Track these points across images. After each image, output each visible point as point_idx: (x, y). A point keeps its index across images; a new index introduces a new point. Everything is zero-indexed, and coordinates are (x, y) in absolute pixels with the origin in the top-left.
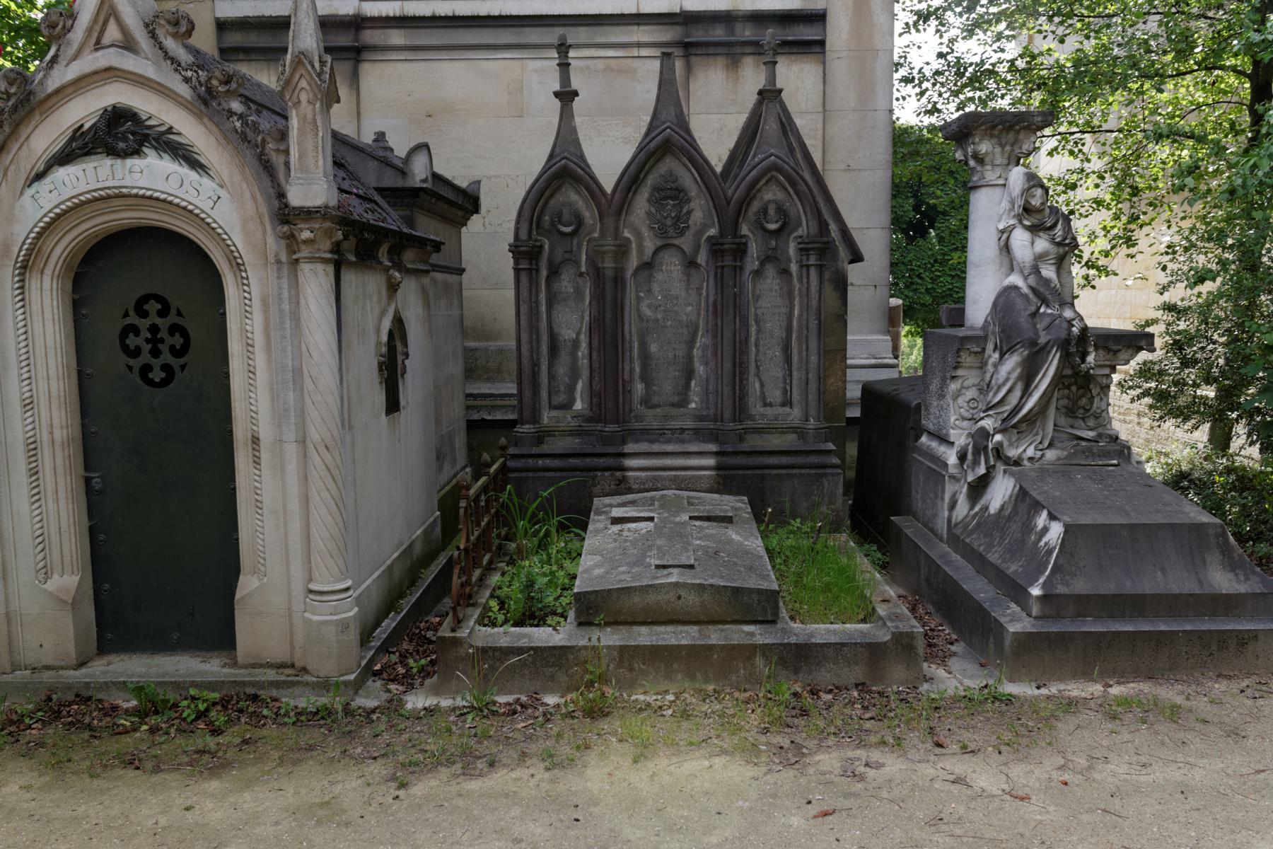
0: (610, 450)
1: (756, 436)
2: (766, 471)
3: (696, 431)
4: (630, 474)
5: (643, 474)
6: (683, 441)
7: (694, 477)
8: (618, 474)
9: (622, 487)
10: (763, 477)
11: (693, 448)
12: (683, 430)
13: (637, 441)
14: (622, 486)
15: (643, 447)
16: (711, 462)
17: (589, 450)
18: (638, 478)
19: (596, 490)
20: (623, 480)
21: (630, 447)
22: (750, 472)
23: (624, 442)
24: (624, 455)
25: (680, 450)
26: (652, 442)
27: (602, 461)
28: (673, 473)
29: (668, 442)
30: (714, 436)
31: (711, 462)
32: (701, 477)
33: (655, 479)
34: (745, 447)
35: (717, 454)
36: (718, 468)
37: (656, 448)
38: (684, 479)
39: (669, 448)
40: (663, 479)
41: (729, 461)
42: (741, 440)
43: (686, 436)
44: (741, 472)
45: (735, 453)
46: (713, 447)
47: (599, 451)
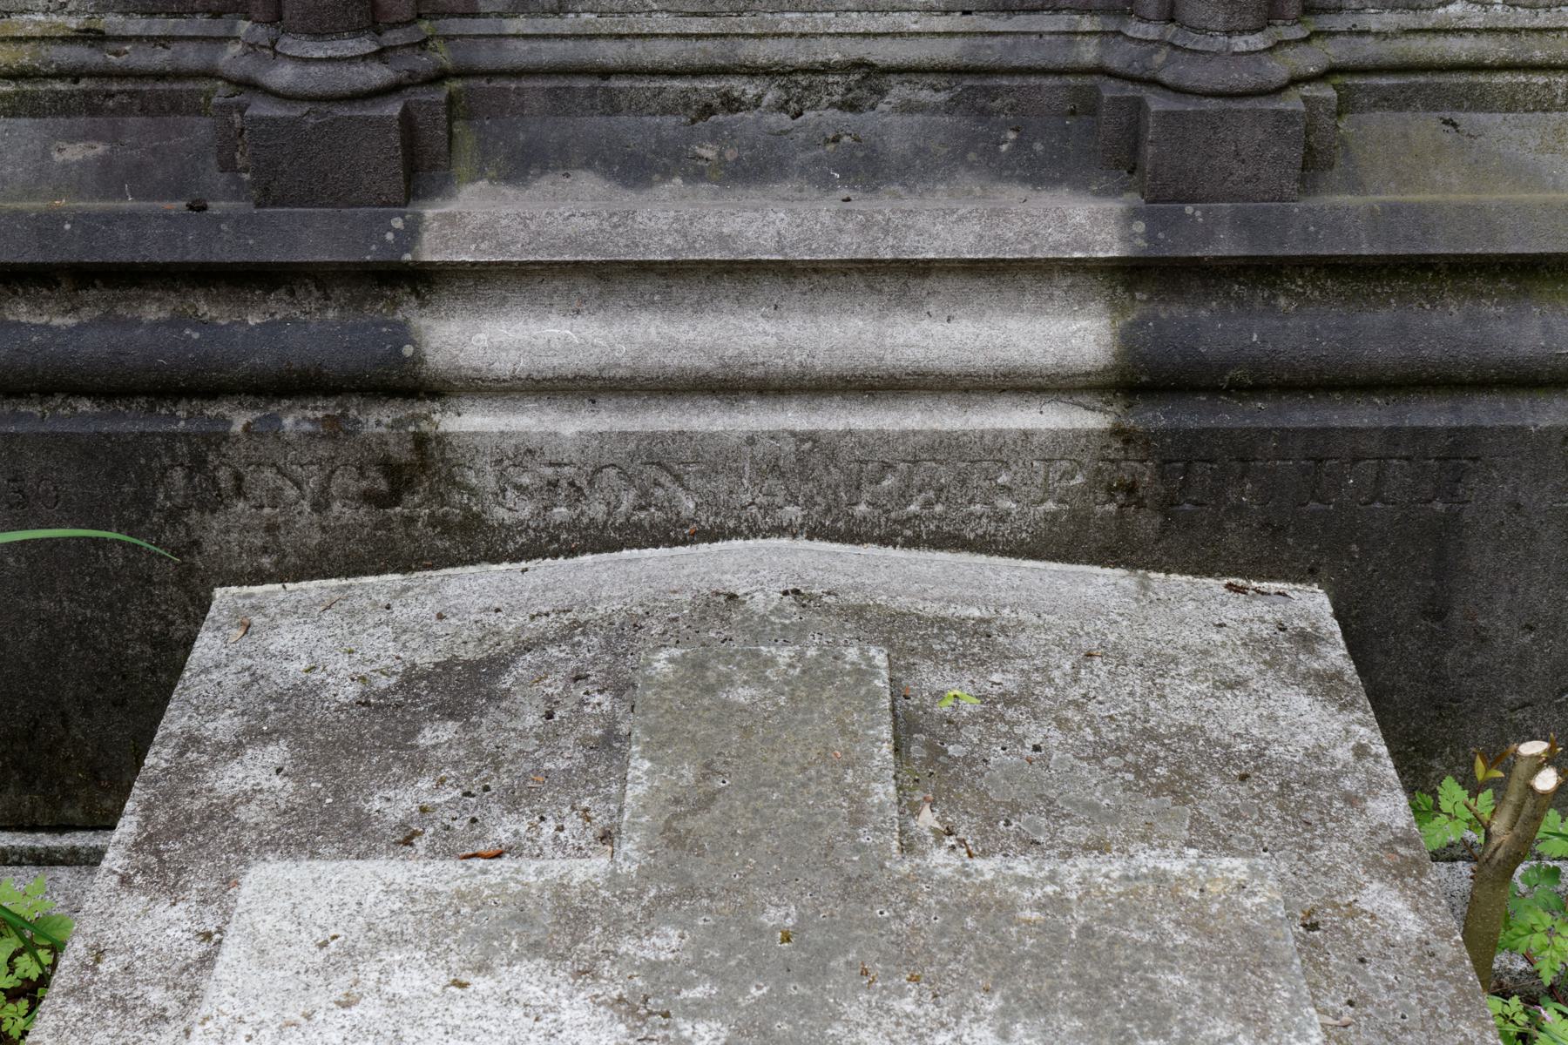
0: (313, 237)
1: (1423, 126)
2: (1483, 411)
3: (968, 79)
4: (468, 422)
5: (569, 426)
6: (864, 168)
7: (944, 446)
8: (378, 420)
9: (413, 513)
10: (1459, 453)
11: (945, 224)
12: (872, 75)
13: (522, 165)
14: (416, 505)
15: (567, 212)
16: (1080, 335)
17: (154, 227)
18: (526, 453)
19: (227, 530)
20: (417, 468)
21: (468, 218)
22: (1365, 415)
23: (420, 170)
24: (426, 281)
25: (850, 246)
26: (634, 169)
27: (251, 326)
28: (793, 418)
29: (754, 169)
30: (1095, 129)
31: (1080, 335)
32: (998, 450)
33: (659, 456)
34: (1343, 217)
35: (1127, 274)
36: (1127, 383)
37: (665, 219)
38: (875, 457)
39: (764, 223)
40: (716, 459)
41: (1220, 328)
42: (1314, 161)
43: (889, 122)
44: (1301, 416)
45: (1264, 272)
46: (1091, 222)
47: (225, 251)
